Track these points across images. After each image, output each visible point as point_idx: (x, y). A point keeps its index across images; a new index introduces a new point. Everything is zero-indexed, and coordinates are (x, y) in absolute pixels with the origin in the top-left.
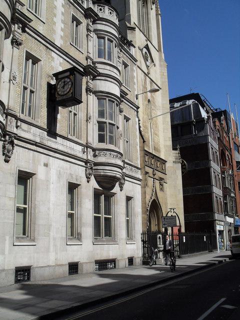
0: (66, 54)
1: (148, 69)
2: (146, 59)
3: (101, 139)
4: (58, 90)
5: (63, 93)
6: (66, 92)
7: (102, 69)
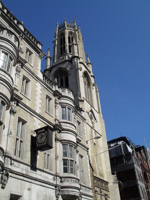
0: (43, 118)
1: (93, 124)
2: (91, 118)
3: (65, 170)
4: (38, 140)
5: (40, 142)
6: (42, 142)
7: (64, 126)
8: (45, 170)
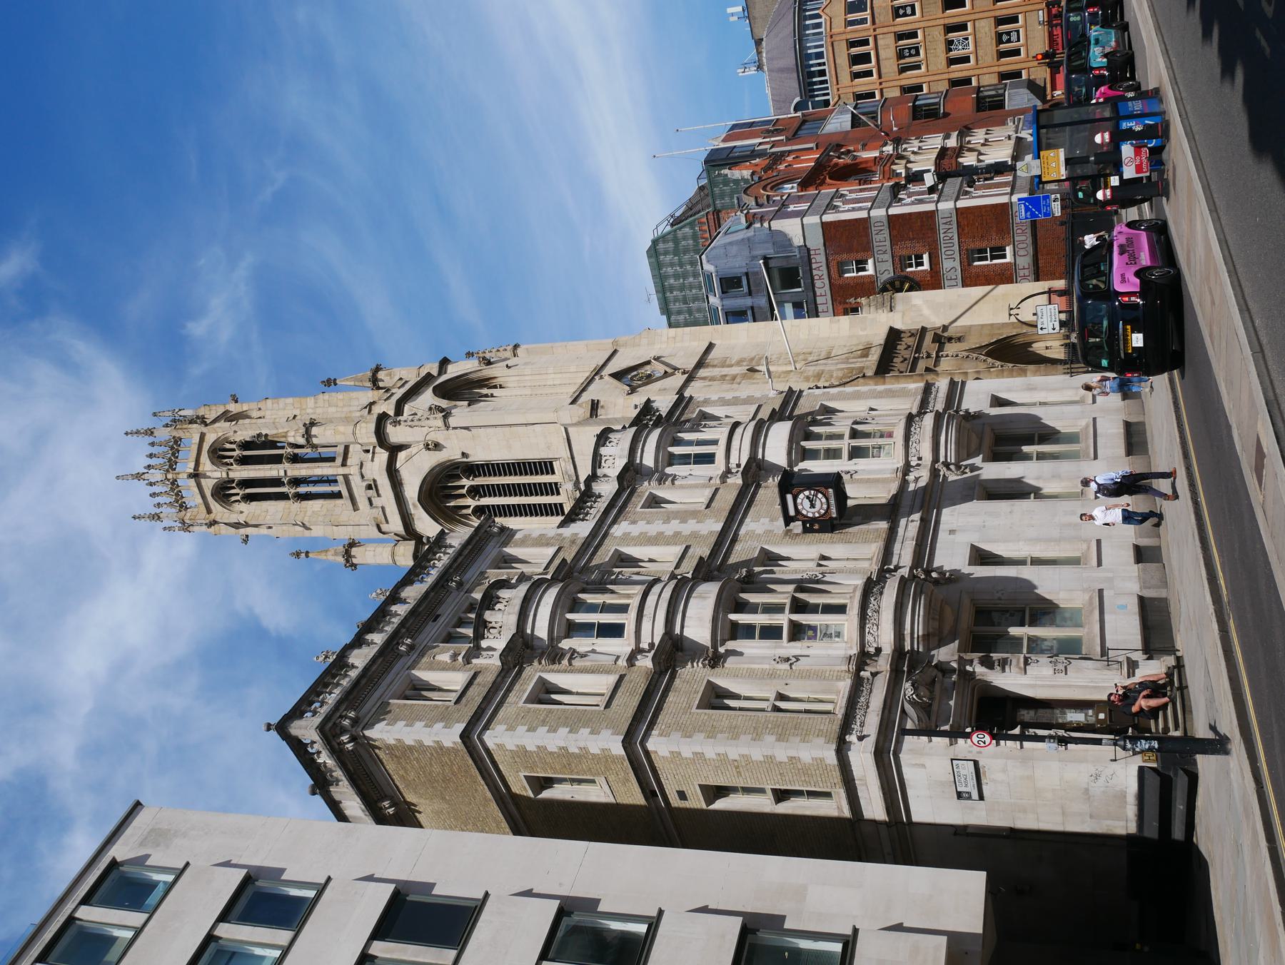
2: (649, 379)
4: (817, 515)
5: (825, 506)
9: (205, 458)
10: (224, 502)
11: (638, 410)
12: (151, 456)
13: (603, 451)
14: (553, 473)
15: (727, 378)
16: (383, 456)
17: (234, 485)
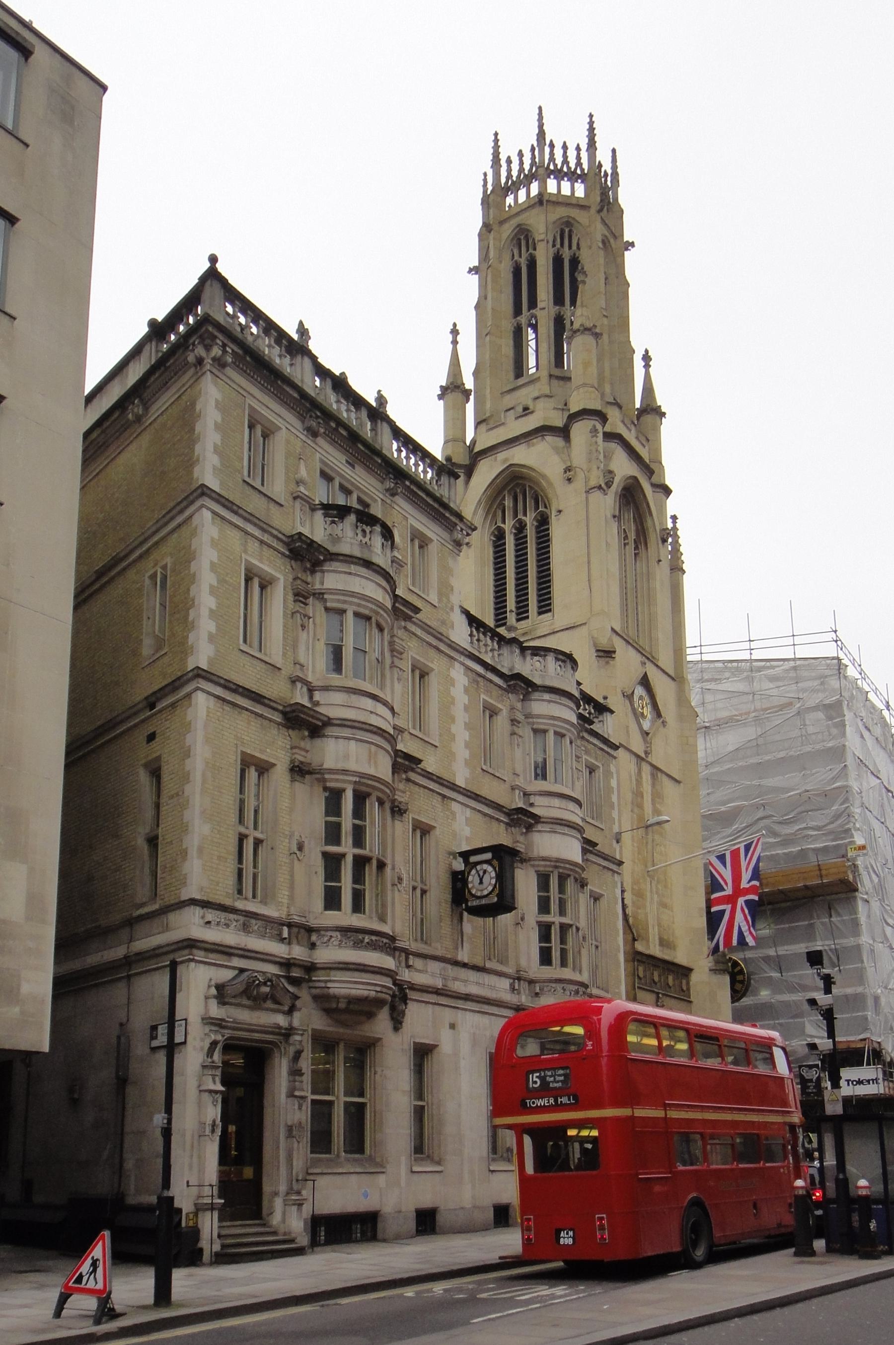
0: (476, 797)
1: (645, 741)
3: (546, 958)
4: (470, 886)
5: (479, 894)
6: (485, 892)
7: (543, 807)
8: (488, 965)
9: (562, 212)
10: (513, 239)
11: (601, 701)
12: (565, 147)
13: (550, 658)
14: (540, 613)
15: (639, 799)
16: (558, 421)
17: (531, 251)
